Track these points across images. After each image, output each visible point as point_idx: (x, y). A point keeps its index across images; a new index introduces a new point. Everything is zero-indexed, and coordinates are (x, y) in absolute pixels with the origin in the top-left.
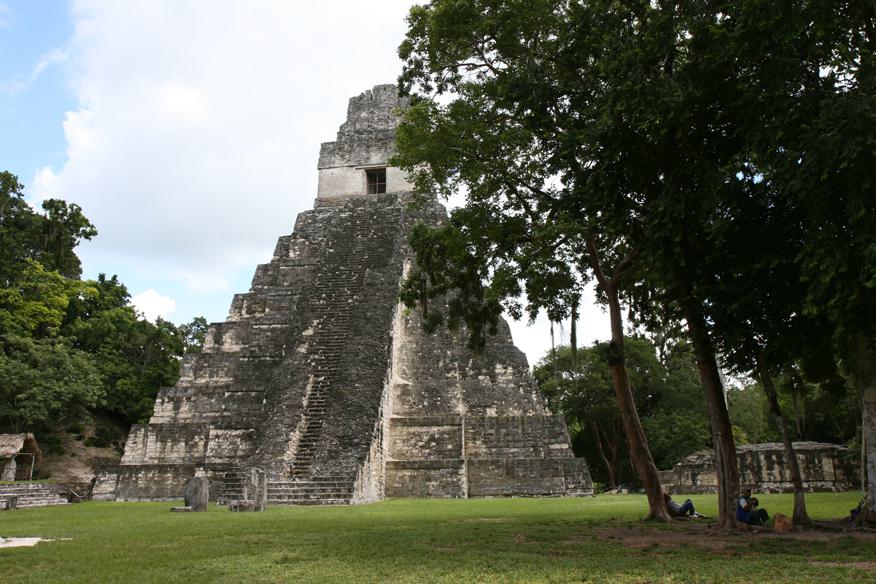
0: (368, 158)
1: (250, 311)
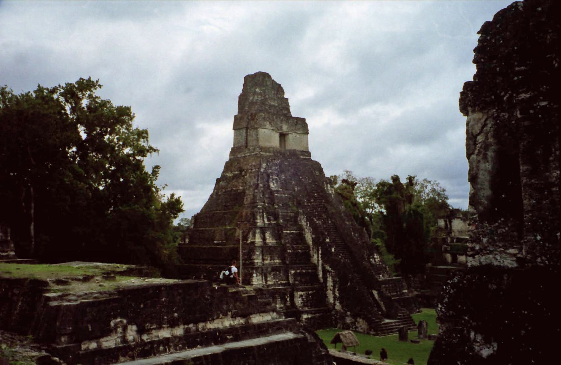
0: (281, 127)
1: (269, 220)
